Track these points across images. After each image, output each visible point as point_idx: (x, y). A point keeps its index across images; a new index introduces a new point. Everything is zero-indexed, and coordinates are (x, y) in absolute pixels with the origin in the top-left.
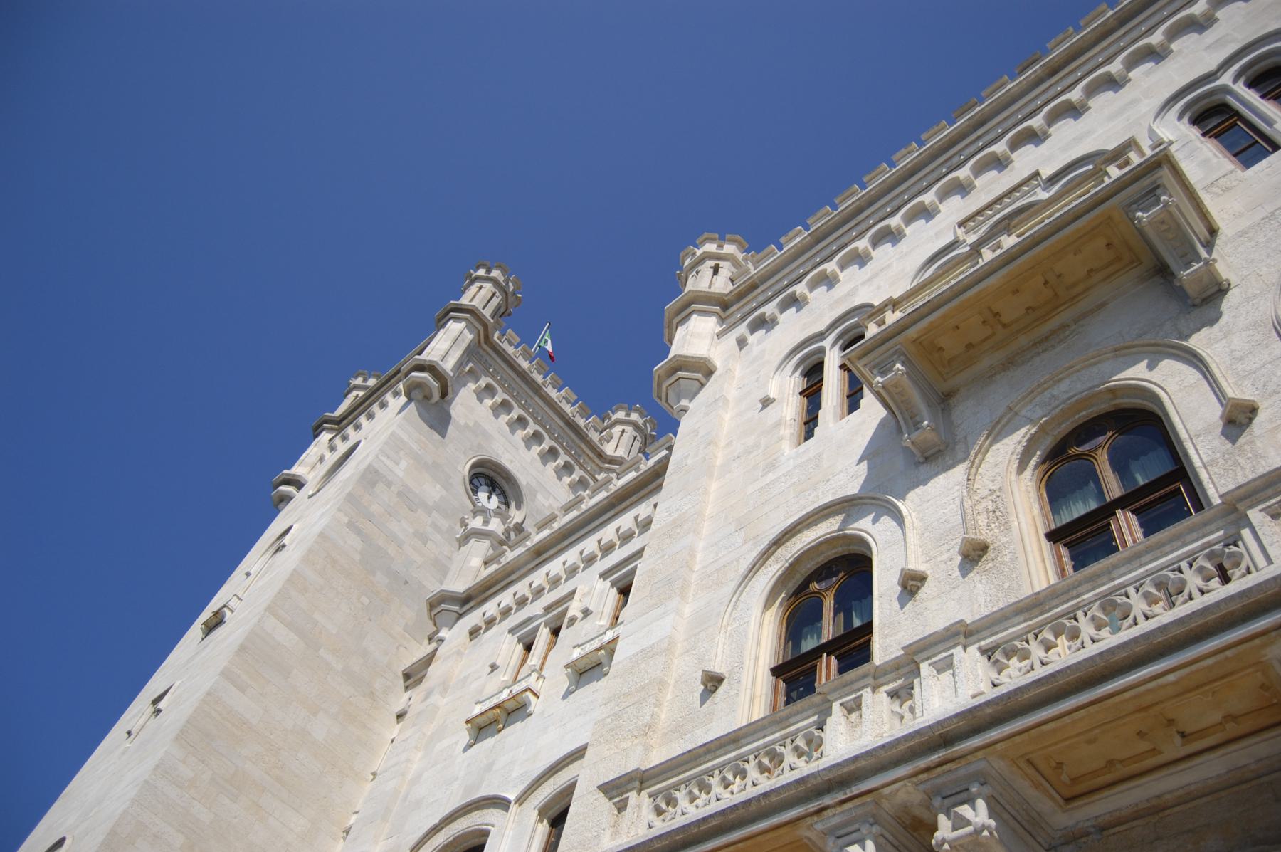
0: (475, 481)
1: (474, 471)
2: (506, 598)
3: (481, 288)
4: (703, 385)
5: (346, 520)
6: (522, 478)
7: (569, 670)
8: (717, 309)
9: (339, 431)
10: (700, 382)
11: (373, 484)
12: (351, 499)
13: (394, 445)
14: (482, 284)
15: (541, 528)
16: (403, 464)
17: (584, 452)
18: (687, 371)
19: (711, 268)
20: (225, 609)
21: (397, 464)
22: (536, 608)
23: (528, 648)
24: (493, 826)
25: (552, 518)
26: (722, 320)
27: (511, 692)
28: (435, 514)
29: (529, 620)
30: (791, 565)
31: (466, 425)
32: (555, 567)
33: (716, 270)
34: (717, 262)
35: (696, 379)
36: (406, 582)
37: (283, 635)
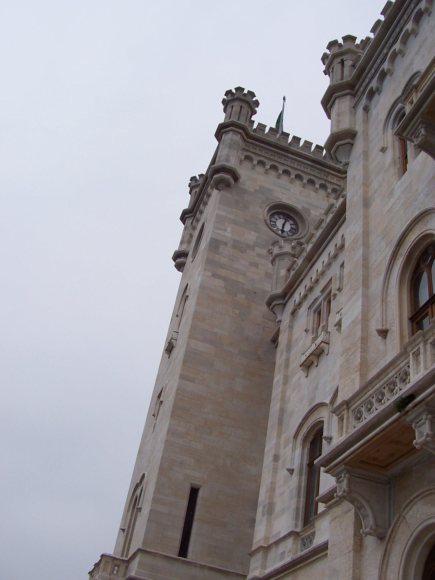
0: (273, 219)
1: (269, 215)
2: (301, 290)
3: (233, 107)
4: (352, 145)
5: (210, 274)
6: (299, 207)
7: (337, 327)
8: (348, 91)
9: (194, 216)
10: (350, 144)
11: (217, 247)
12: (209, 262)
13: (220, 220)
14: (233, 104)
15: (317, 229)
16: (229, 229)
17: (329, 173)
18: (342, 140)
19: (339, 63)
20: (172, 340)
21: (225, 230)
22: (317, 292)
23: (319, 313)
24: (324, 417)
25: (322, 221)
26: (354, 95)
27: (316, 345)
28: (256, 248)
29: (316, 300)
30: (407, 256)
31: (256, 191)
32: (319, 266)
33: (342, 62)
34: (341, 58)
35: (347, 143)
36: (255, 293)
37: (202, 347)
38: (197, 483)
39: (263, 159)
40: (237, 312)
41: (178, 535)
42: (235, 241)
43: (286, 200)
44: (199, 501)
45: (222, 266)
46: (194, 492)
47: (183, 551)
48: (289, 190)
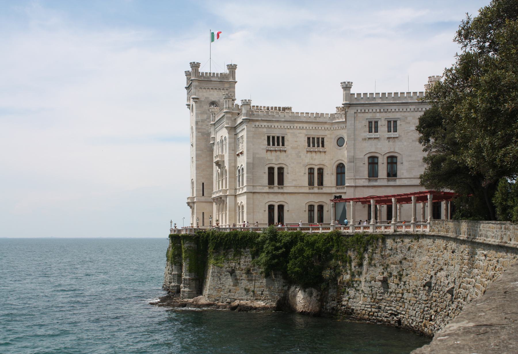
5: (197, 132)
16: (199, 117)
21: (199, 117)
28: (207, 120)
39: (204, 87)
41: (202, 192)
42: (202, 120)
43: (213, 99)
44: (204, 185)
45: (199, 129)
46: (203, 184)
47: (203, 195)
48: (213, 95)
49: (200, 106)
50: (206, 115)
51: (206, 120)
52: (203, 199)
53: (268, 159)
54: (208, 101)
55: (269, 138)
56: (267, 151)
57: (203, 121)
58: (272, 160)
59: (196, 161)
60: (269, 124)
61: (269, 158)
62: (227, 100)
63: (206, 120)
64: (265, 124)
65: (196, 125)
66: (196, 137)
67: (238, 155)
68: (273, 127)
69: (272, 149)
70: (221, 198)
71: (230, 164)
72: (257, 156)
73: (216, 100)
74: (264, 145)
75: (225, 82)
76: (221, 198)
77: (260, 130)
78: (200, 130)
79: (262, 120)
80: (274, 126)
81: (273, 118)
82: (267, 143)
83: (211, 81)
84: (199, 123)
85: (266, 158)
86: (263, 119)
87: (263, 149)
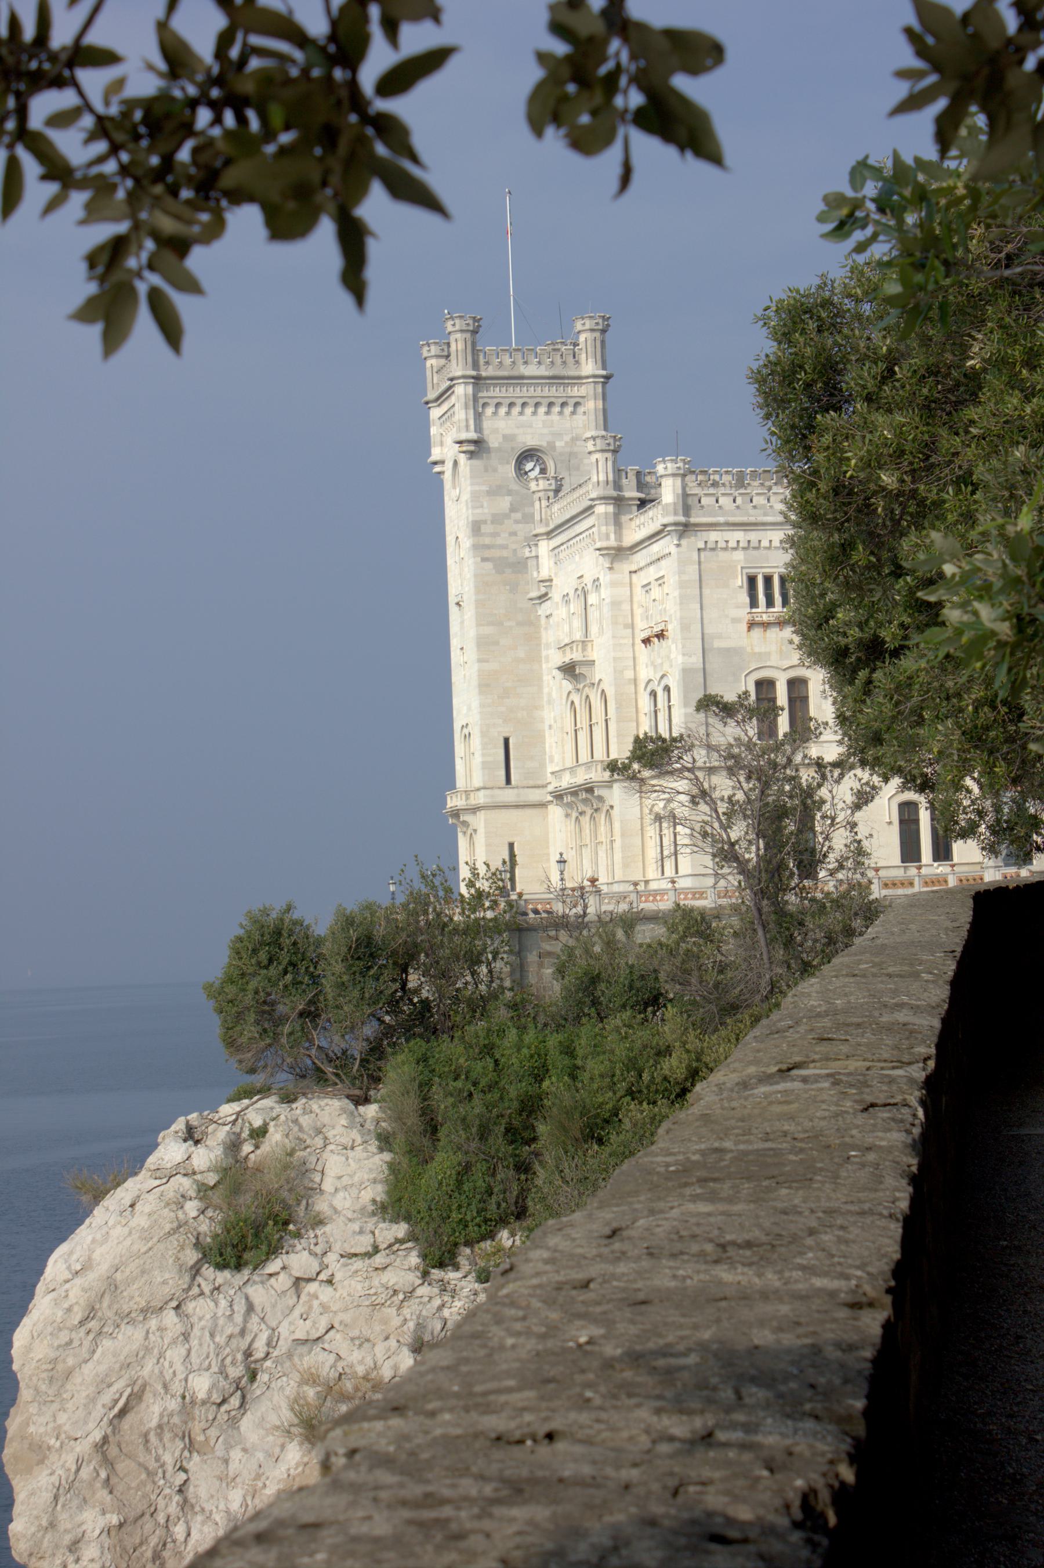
5: (479, 559)
13: (475, 497)
16: (485, 504)
21: (482, 507)
28: (513, 515)
38: (506, 735)
40: (508, 587)
41: (503, 772)
42: (494, 515)
43: (530, 441)
45: (488, 547)
46: (506, 741)
48: (531, 426)
49: (486, 470)
50: (508, 499)
51: (507, 516)
52: (508, 795)
53: (755, 654)
54: (513, 449)
55: (752, 581)
56: (752, 625)
57: (497, 519)
58: (769, 654)
59: (480, 661)
60: (753, 536)
61: (757, 650)
62: (598, 456)
63: (507, 516)
64: (739, 535)
65: (474, 536)
66: (476, 576)
67: (646, 641)
68: (765, 543)
69: (765, 618)
70: (590, 790)
71: (618, 672)
72: (717, 644)
73: (538, 443)
74: (738, 607)
75: (569, 378)
76: (590, 790)
77: (723, 555)
78: (487, 554)
79: (727, 524)
80: (771, 541)
81: (765, 514)
82: (747, 600)
83: (522, 378)
84: (485, 529)
85: (749, 649)
86: (732, 519)
87: (735, 620)
